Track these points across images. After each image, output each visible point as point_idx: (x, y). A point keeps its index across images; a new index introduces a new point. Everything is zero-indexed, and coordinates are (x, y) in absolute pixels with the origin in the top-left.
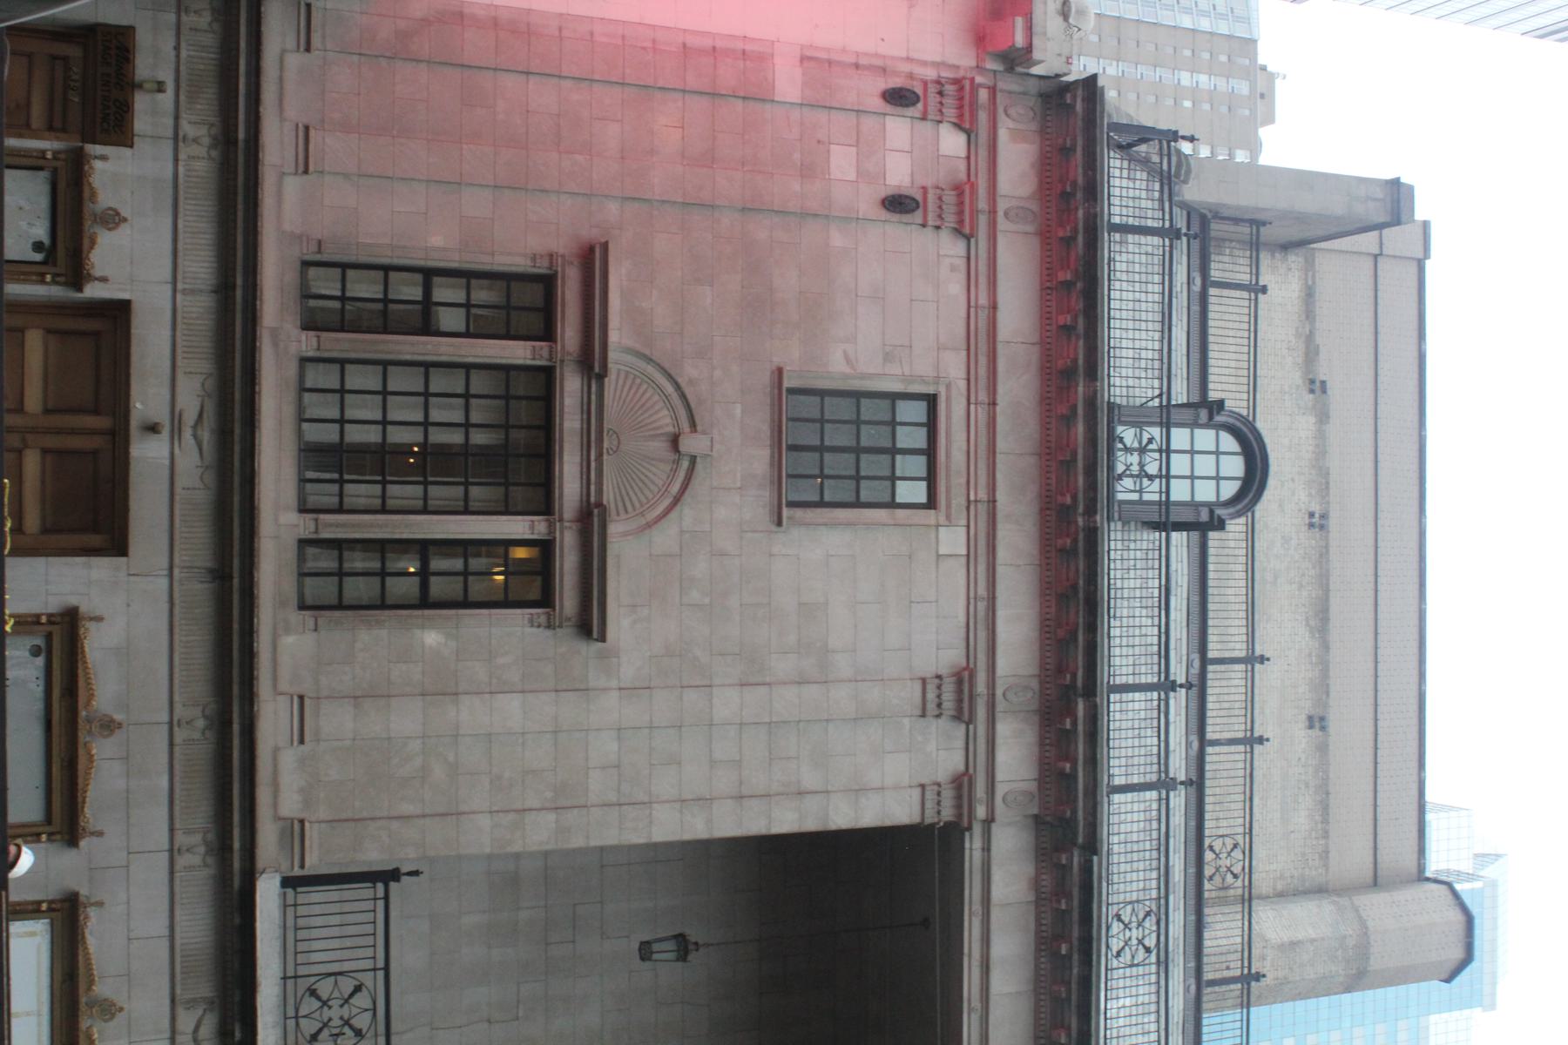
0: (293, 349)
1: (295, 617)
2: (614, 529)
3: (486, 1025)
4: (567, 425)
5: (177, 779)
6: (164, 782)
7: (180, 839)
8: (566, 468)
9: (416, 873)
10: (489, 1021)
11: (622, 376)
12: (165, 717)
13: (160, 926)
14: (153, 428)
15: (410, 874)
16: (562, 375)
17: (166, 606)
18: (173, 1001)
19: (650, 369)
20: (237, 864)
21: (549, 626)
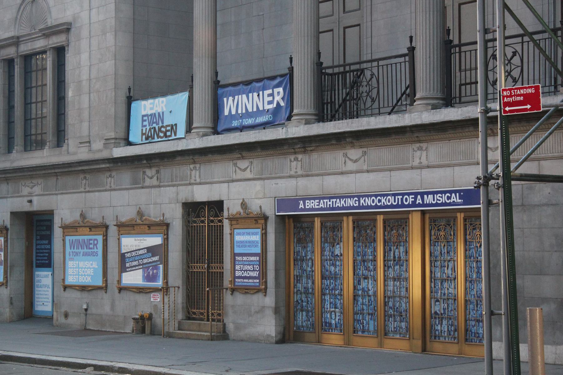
0: (15, 155)
1: (65, 148)
2: (49, 24)
3: (264, 30)
4: (30, 48)
5: (97, 189)
6: (97, 193)
7: (108, 187)
8: (38, 46)
9: (130, 89)
10: (263, 29)
11: (21, 28)
12: (84, 194)
13: (125, 192)
14: (30, 201)
15: (130, 92)
16: (23, 52)
17: (64, 195)
18: (143, 188)
19: (19, 17)
20: (108, 165)
21: (68, 45)
